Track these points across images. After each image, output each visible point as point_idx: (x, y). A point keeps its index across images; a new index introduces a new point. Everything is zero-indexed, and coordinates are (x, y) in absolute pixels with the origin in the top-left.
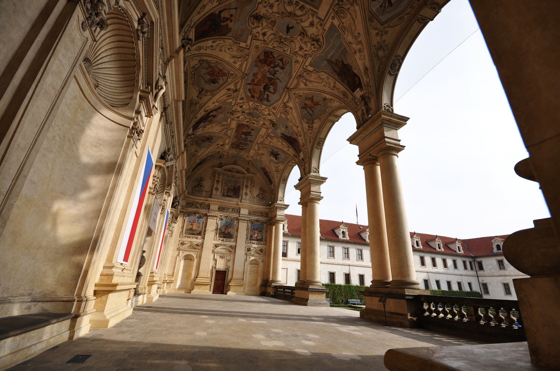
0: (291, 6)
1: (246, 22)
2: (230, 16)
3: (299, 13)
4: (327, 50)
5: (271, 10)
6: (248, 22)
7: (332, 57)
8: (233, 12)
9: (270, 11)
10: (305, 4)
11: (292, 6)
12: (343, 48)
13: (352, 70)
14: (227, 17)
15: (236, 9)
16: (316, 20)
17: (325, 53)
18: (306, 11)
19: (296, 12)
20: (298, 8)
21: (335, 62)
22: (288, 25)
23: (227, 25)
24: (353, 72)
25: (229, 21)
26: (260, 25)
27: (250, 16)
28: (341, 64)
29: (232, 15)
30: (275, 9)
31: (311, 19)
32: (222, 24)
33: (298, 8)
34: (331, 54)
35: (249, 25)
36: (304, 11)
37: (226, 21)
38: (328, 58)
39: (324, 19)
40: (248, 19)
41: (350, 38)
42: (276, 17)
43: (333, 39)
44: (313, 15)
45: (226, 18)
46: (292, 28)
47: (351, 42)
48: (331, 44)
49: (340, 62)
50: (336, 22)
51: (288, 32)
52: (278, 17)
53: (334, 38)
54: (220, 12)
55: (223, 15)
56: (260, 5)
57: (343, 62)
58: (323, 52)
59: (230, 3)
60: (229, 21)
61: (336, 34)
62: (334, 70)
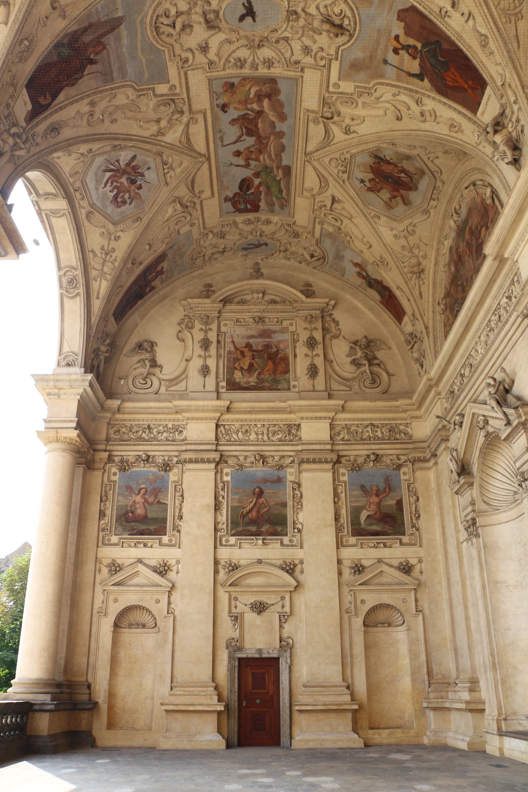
0: (265, 60)
1: (360, 21)
2: (401, 52)
3: (243, 53)
4: (139, 35)
5: (304, 42)
6: (356, 24)
7: (118, 39)
8: (391, 57)
9: (307, 41)
10: (238, 71)
11: (262, 60)
12: (115, 74)
13: (67, 85)
14: (407, 55)
15: (386, 62)
16: (200, 58)
17: (138, 26)
18: (229, 62)
19: (249, 51)
20: (249, 61)
21: (103, 40)
22: (254, 21)
23: (407, 34)
24: (61, 89)
25: (403, 39)
26: (322, 10)
27: (351, 36)
28: (92, 56)
29: (396, 51)
30: (297, 46)
31: (212, 55)
32: (419, 45)
33: (249, 61)
34: (125, 41)
35: (354, 17)
36: (233, 61)
37: (409, 46)
38: (123, 27)
39: (186, 74)
40: (355, 30)
41: (121, 99)
42: (288, 29)
43: (144, 63)
44: (211, 63)
45: (410, 54)
46: (242, 18)
47: (113, 101)
48: (140, 54)
49: (97, 54)
50: (162, 89)
51: (246, 4)
52: (285, 30)
53: (145, 66)
54: (420, 77)
55: (415, 66)
56: (332, 52)
57: (92, 62)
58: (142, 22)
59: (398, 80)
60: (402, 39)
61: (146, 75)
62: (91, 25)
